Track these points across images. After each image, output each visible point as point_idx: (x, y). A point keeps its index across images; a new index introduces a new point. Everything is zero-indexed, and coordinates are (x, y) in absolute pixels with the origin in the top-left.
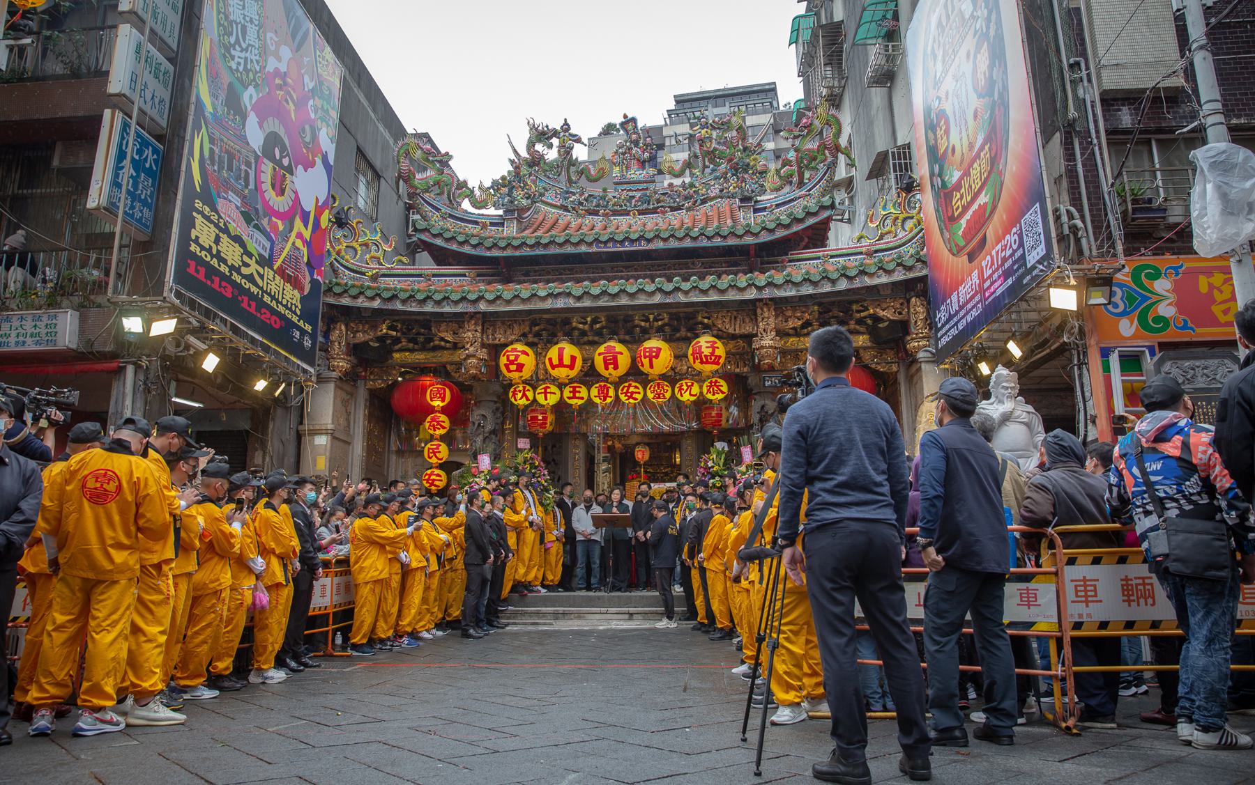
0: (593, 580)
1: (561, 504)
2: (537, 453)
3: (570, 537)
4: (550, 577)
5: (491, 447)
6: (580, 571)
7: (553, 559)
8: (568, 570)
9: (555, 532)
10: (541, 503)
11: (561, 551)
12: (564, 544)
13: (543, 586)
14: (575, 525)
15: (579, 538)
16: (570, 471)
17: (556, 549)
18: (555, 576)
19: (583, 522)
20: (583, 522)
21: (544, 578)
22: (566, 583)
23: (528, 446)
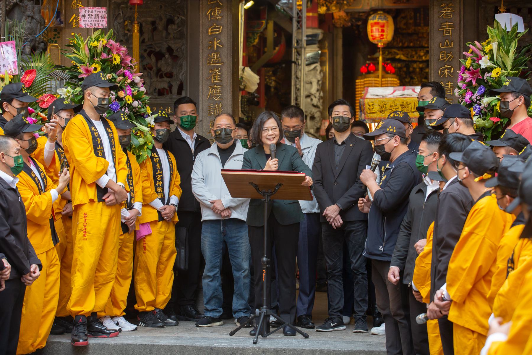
0: (237, 304)
1: (172, 143)
2: (125, 39)
3: (189, 210)
4: (146, 295)
5: (22, 27)
6: (210, 284)
7: (151, 258)
8: (187, 281)
9: (158, 204)
10: (126, 147)
11: (171, 243)
12: (178, 227)
13: (133, 315)
14: (199, 189)
15: (207, 215)
16: (203, 72)
17: (160, 241)
18: (157, 292)
19: (211, 183)
20: (211, 183)
21: (133, 296)
22: (183, 306)
23: (103, 23)
